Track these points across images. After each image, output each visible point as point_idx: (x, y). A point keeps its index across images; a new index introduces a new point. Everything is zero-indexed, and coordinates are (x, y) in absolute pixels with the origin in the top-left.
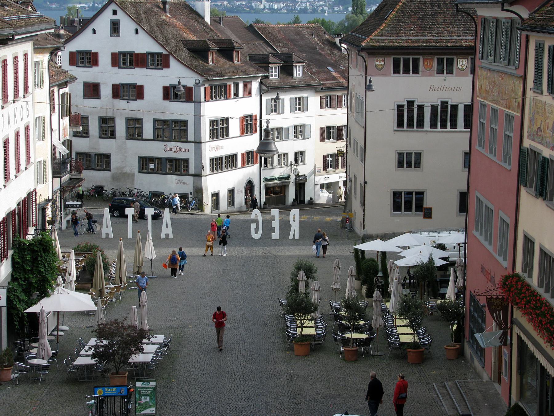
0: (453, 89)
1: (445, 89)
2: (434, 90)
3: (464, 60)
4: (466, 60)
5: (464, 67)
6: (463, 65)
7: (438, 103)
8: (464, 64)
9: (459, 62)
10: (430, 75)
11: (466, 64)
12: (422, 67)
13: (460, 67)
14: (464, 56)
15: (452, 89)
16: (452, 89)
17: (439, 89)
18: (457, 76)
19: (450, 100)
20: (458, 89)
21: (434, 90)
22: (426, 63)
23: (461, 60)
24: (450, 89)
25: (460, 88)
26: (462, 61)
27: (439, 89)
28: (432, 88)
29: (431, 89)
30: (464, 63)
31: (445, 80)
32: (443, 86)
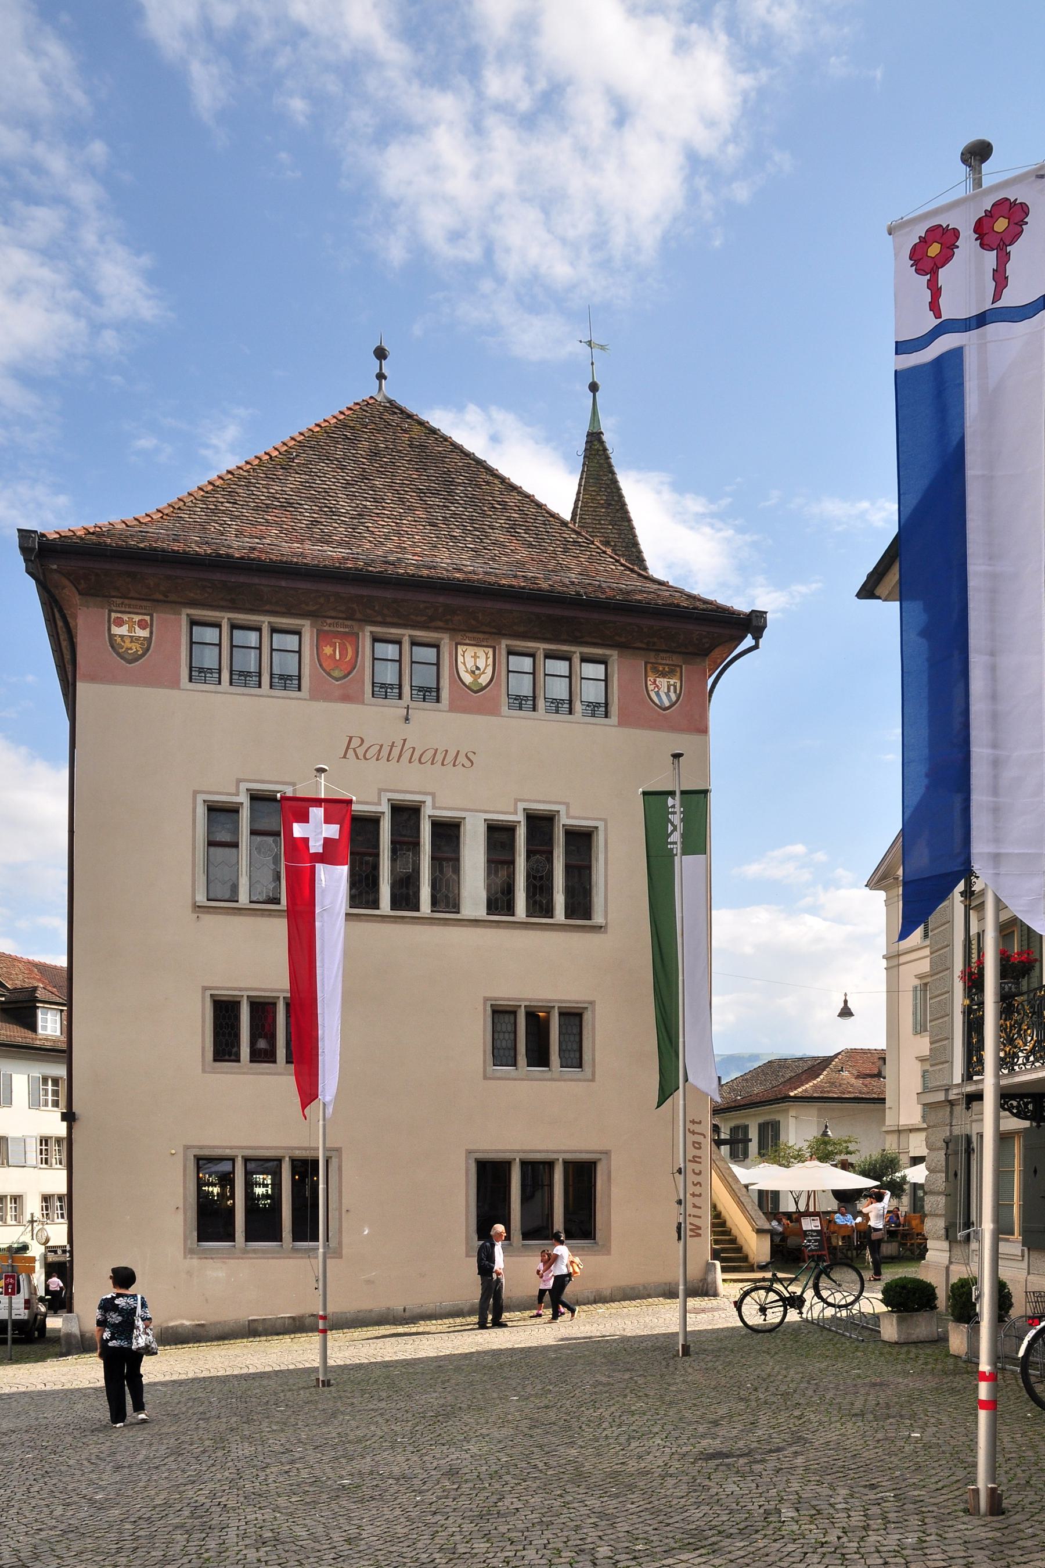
0: (439, 757)
1: (406, 755)
2: (361, 756)
3: (481, 652)
4: (490, 651)
5: (484, 680)
6: (478, 668)
7: (379, 809)
8: (482, 666)
9: (460, 659)
10: (346, 698)
11: (489, 671)
12: (311, 655)
13: (468, 679)
14: (481, 636)
15: (436, 758)
16: (436, 758)
17: (385, 753)
18: (453, 708)
19: (429, 800)
20: (462, 759)
21: (361, 756)
22: (328, 650)
23: (470, 651)
24: (429, 754)
25: (470, 755)
26: (475, 657)
27: (385, 753)
28: (352, 748)
29: (351, 751)
30: (481, 664)
31: (407, 719)
32: (399, 743)
